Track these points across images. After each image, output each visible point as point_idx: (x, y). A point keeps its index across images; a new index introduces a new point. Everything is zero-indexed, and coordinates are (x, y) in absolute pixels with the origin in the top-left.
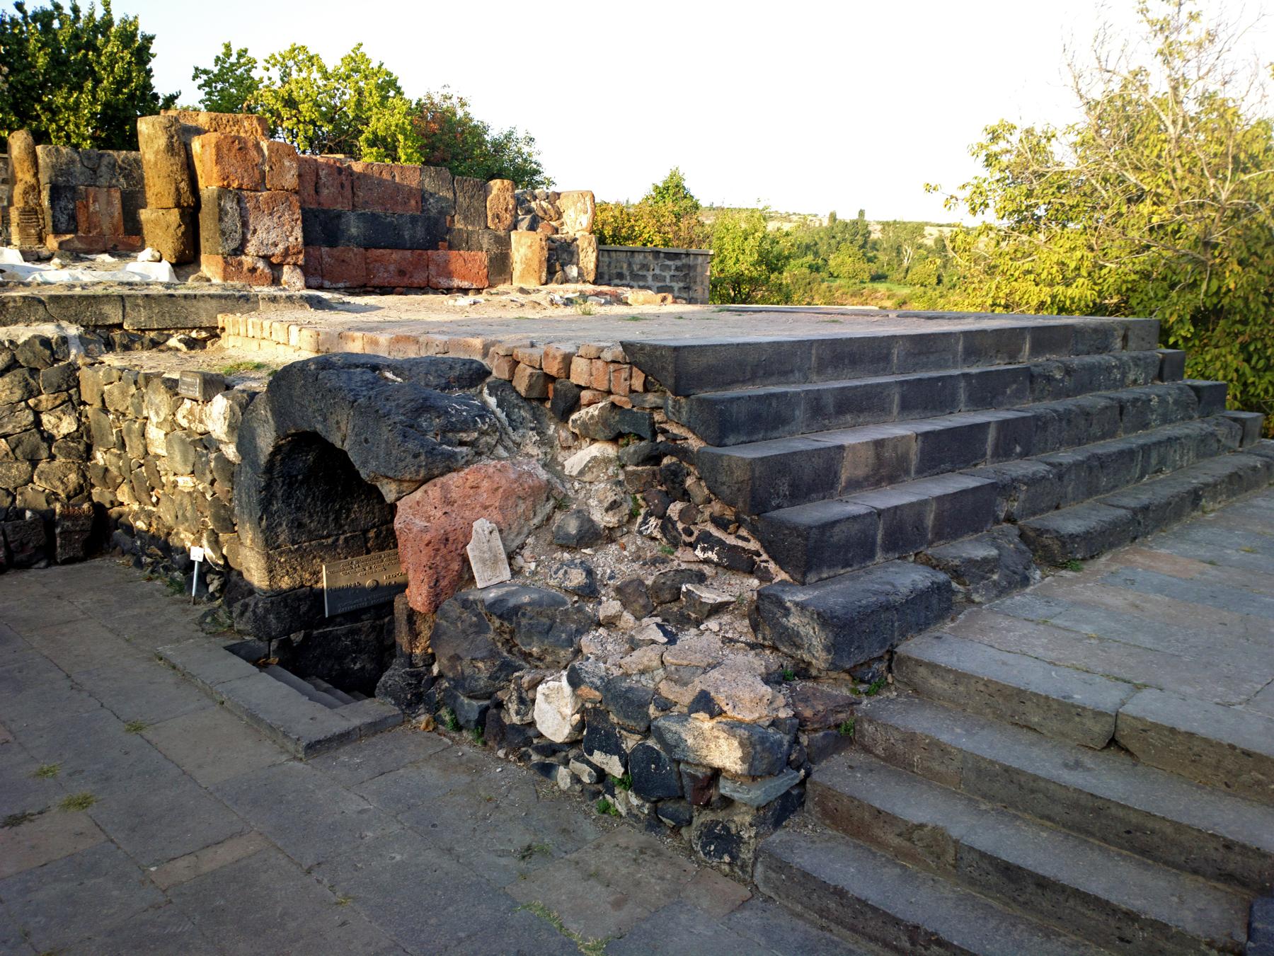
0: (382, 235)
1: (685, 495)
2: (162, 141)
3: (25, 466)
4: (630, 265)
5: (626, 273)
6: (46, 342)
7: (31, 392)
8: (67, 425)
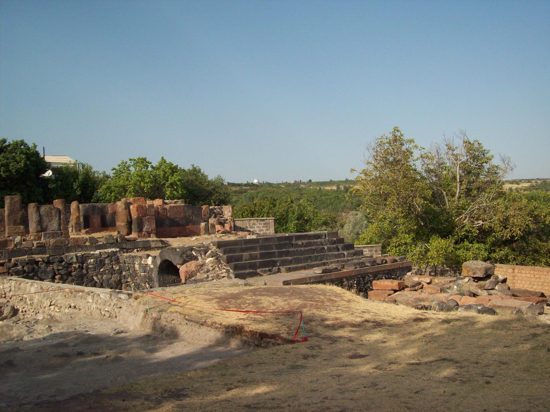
0: (174, 223)
1: (221, 263)
2: (124, 206)
3: (110, 275)
4: (249, 224)
5: (248, 226)
6: (114, 252)
7: (112, 261)
8: (117, 268)
